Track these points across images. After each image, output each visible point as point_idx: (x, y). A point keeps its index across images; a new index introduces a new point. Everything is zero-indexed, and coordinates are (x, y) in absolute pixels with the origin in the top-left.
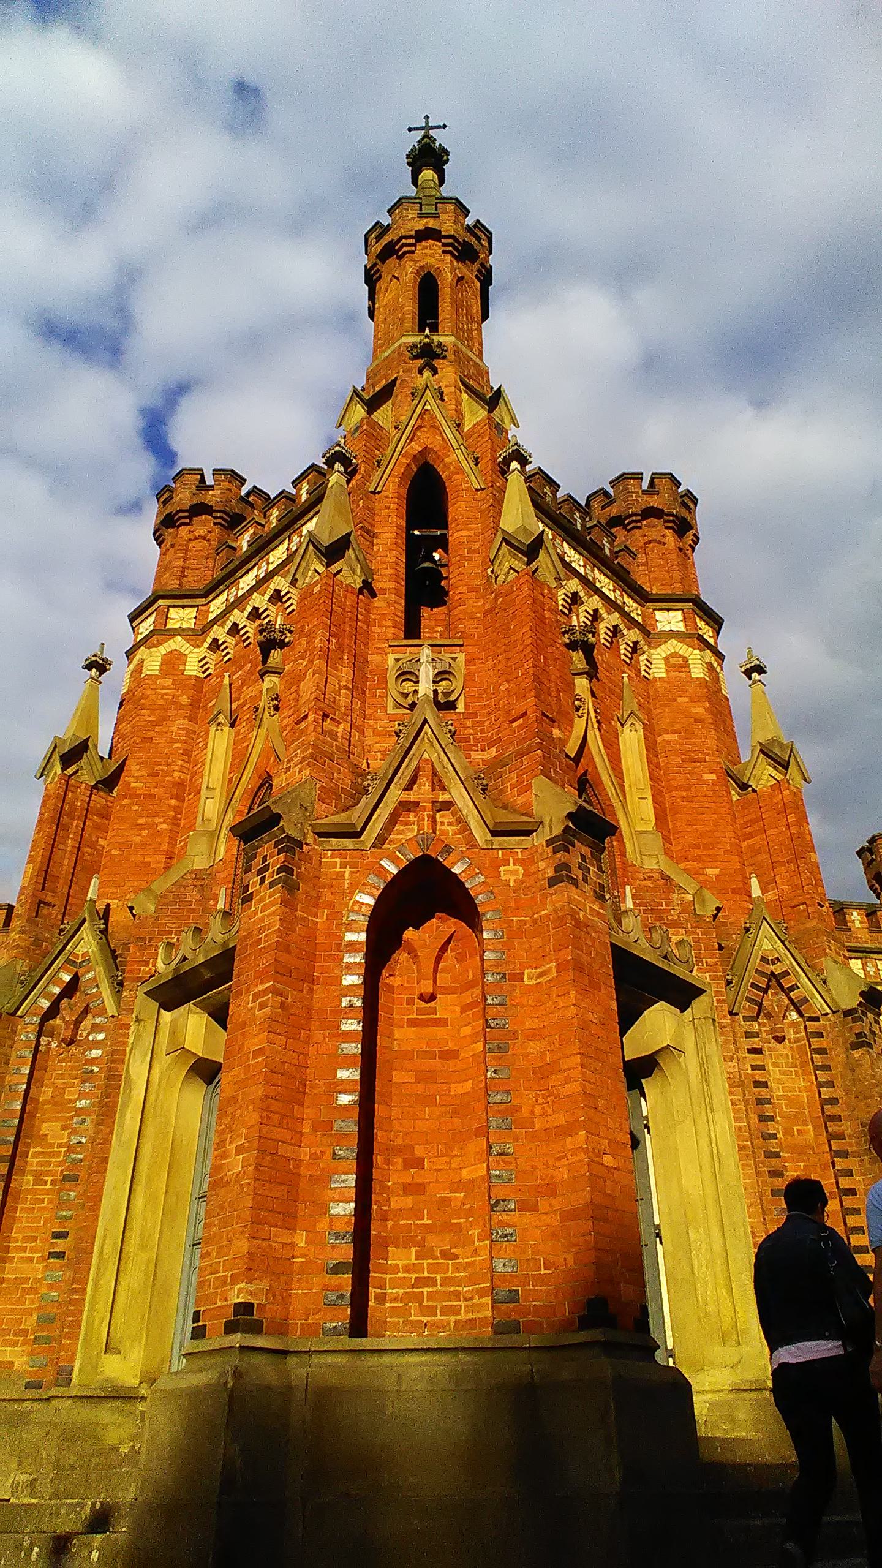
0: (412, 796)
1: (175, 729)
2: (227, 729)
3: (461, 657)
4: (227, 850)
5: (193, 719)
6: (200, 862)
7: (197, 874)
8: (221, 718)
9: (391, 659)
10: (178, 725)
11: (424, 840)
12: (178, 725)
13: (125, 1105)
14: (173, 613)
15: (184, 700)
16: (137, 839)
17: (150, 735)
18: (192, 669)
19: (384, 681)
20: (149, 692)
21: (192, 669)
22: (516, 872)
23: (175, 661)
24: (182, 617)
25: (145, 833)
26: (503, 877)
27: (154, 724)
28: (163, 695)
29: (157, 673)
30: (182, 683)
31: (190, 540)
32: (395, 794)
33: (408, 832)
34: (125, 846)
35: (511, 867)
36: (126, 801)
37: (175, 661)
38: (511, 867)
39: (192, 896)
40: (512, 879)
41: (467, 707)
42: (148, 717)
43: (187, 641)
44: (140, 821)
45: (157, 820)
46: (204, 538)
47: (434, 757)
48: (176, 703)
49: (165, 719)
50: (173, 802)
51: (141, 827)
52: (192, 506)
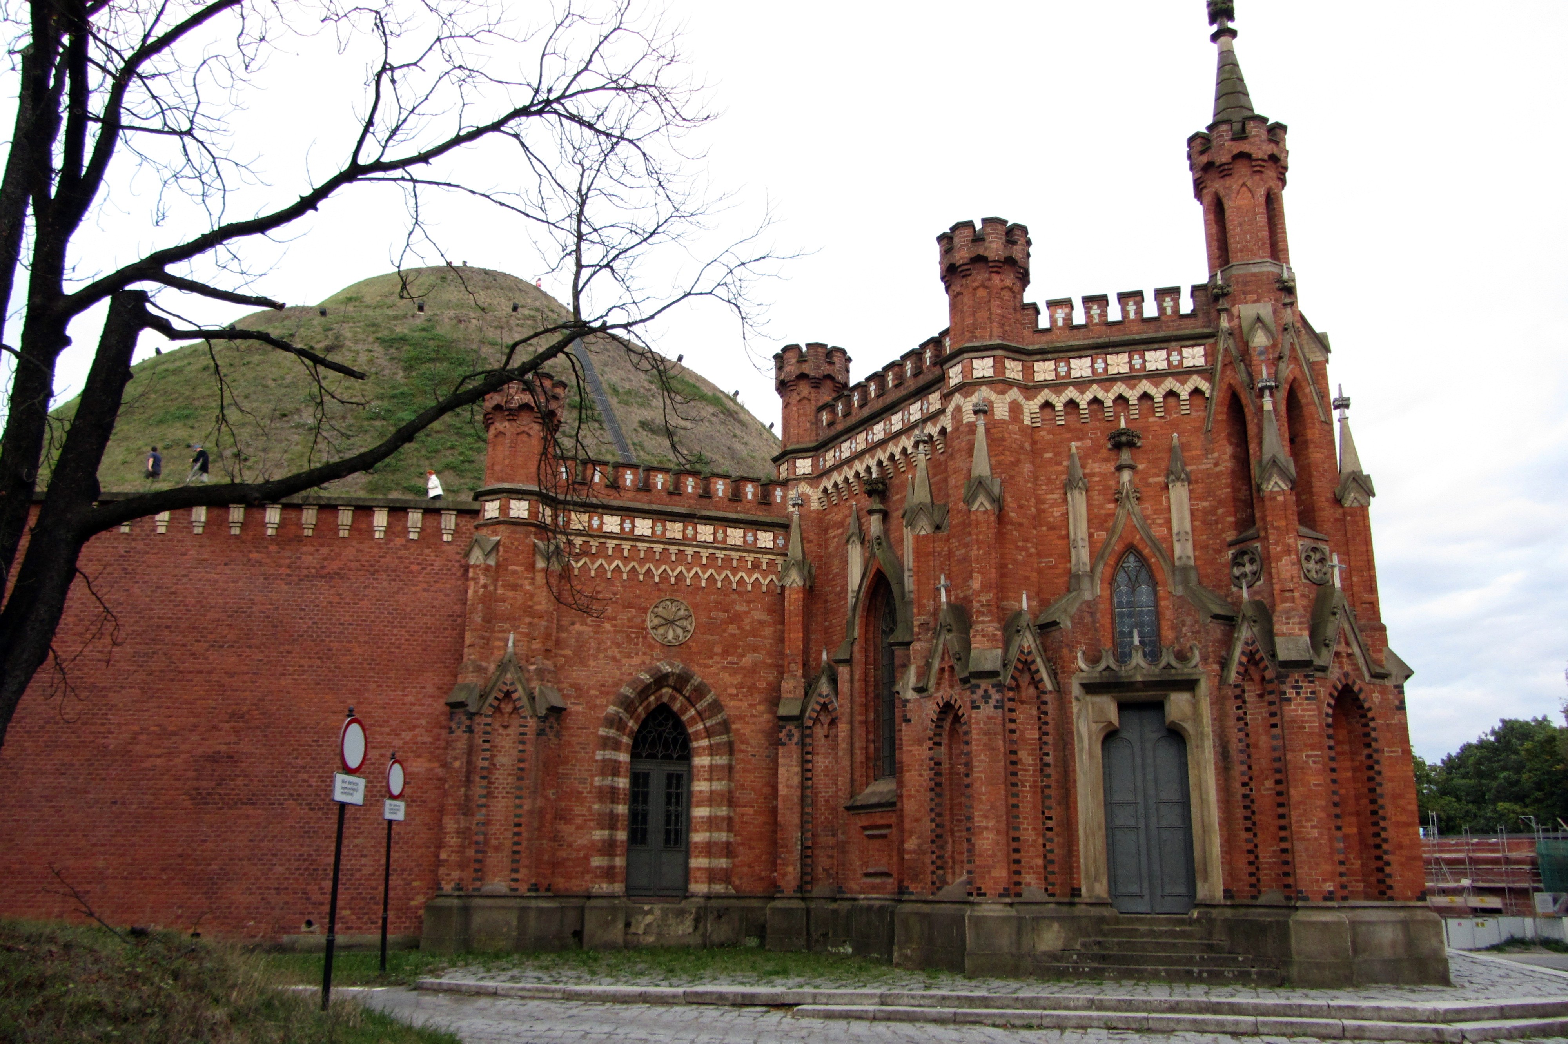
6: (1087, 596)
12: (1027, 468)
13: (1081, 751)
14: (1009, 364)
15: (1027, 446)
23: (1015, 409)
24: (1014, 369)
25: (1023, 553)
29: (1007, 418)
30: (1023, 430)
37: (1015, 409)
39: (1088, 619)
43: (1021, 392)
44: (1020, 544)
45: (1029, 545)
48: (1022, 448)
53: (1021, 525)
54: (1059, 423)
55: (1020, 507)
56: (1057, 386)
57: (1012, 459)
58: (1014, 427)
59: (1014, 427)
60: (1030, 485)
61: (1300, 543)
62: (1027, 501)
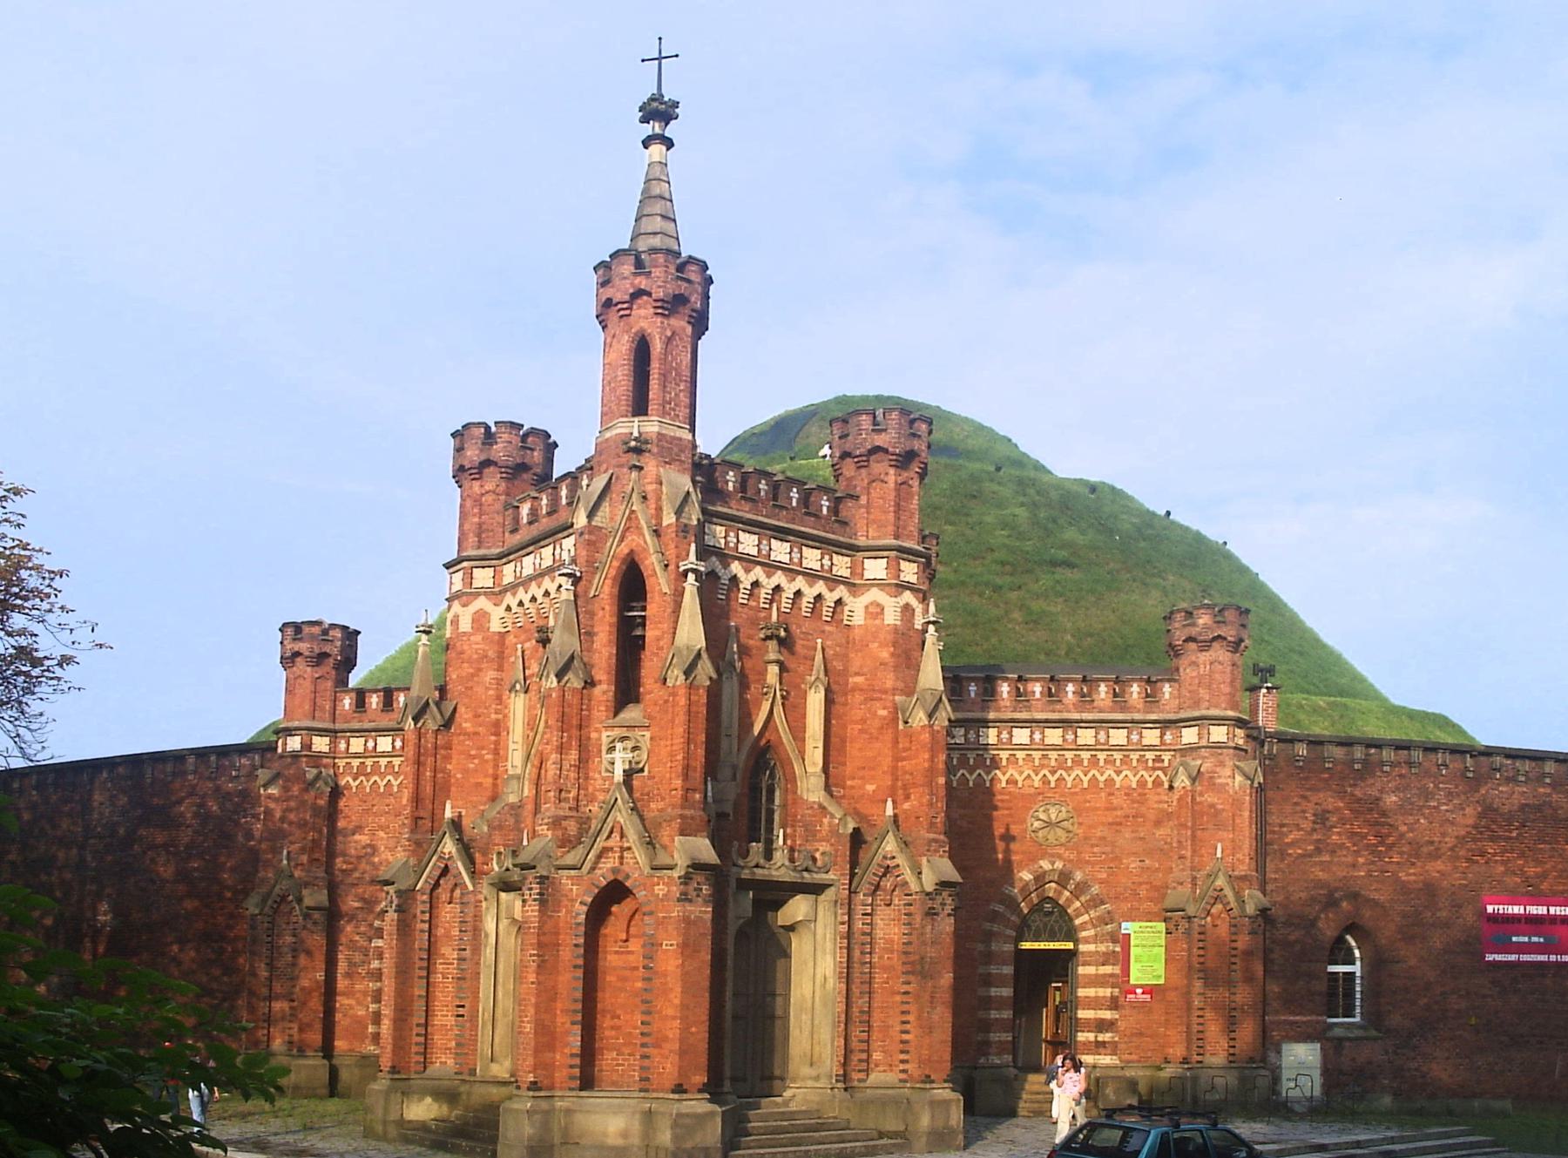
0: (610, 843)
1: (488, 679)
2: (522, 695)
3: (648, 734)
4: (530, 790)
5: (500, 669)
6: (512, 799)
7: (512, 807)
8: (518, 687)
9: (605, 734)
10: (490, 675)
11: (614, 871)
12: (490, 675)
15: (491, 654)
16: (472, 766)
17: (470, 684)
18: (495, 626)
19: (600, 751)
20: (466, 647)
21: (495, 626)
22: (663, 890)
24: (483, 577)
25: (476, 761)
26: (656, 892)
27: (473, 675)
28: (477, 649)
31: (483, 495)
32: (600, 843)
33: (609, 863)
34: (465, 771)
35: (661, 887)
36: (462, 738)
38: (661, 887)
40: (661, 893)
41: (649, 772)
42: (467, 669)
44: (473, 752)
45: (484, 752)
46: (494, 492)
47: (622, 821)
49: (480, 670)
50: (493, 738)
51: (474, 757)
52: (480, 463)
53: (476, 733)
54: (519, 625)
55: (477, 716)
56: (513, 588)
57: (471, 671)
58: (478, 638)
59: (478, 638)
60: (491, 692)
61: (605, 734)
62: (486, 708)
